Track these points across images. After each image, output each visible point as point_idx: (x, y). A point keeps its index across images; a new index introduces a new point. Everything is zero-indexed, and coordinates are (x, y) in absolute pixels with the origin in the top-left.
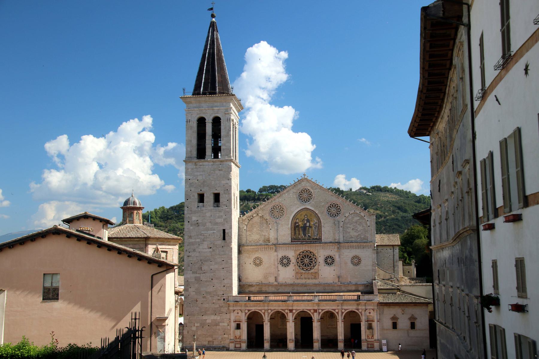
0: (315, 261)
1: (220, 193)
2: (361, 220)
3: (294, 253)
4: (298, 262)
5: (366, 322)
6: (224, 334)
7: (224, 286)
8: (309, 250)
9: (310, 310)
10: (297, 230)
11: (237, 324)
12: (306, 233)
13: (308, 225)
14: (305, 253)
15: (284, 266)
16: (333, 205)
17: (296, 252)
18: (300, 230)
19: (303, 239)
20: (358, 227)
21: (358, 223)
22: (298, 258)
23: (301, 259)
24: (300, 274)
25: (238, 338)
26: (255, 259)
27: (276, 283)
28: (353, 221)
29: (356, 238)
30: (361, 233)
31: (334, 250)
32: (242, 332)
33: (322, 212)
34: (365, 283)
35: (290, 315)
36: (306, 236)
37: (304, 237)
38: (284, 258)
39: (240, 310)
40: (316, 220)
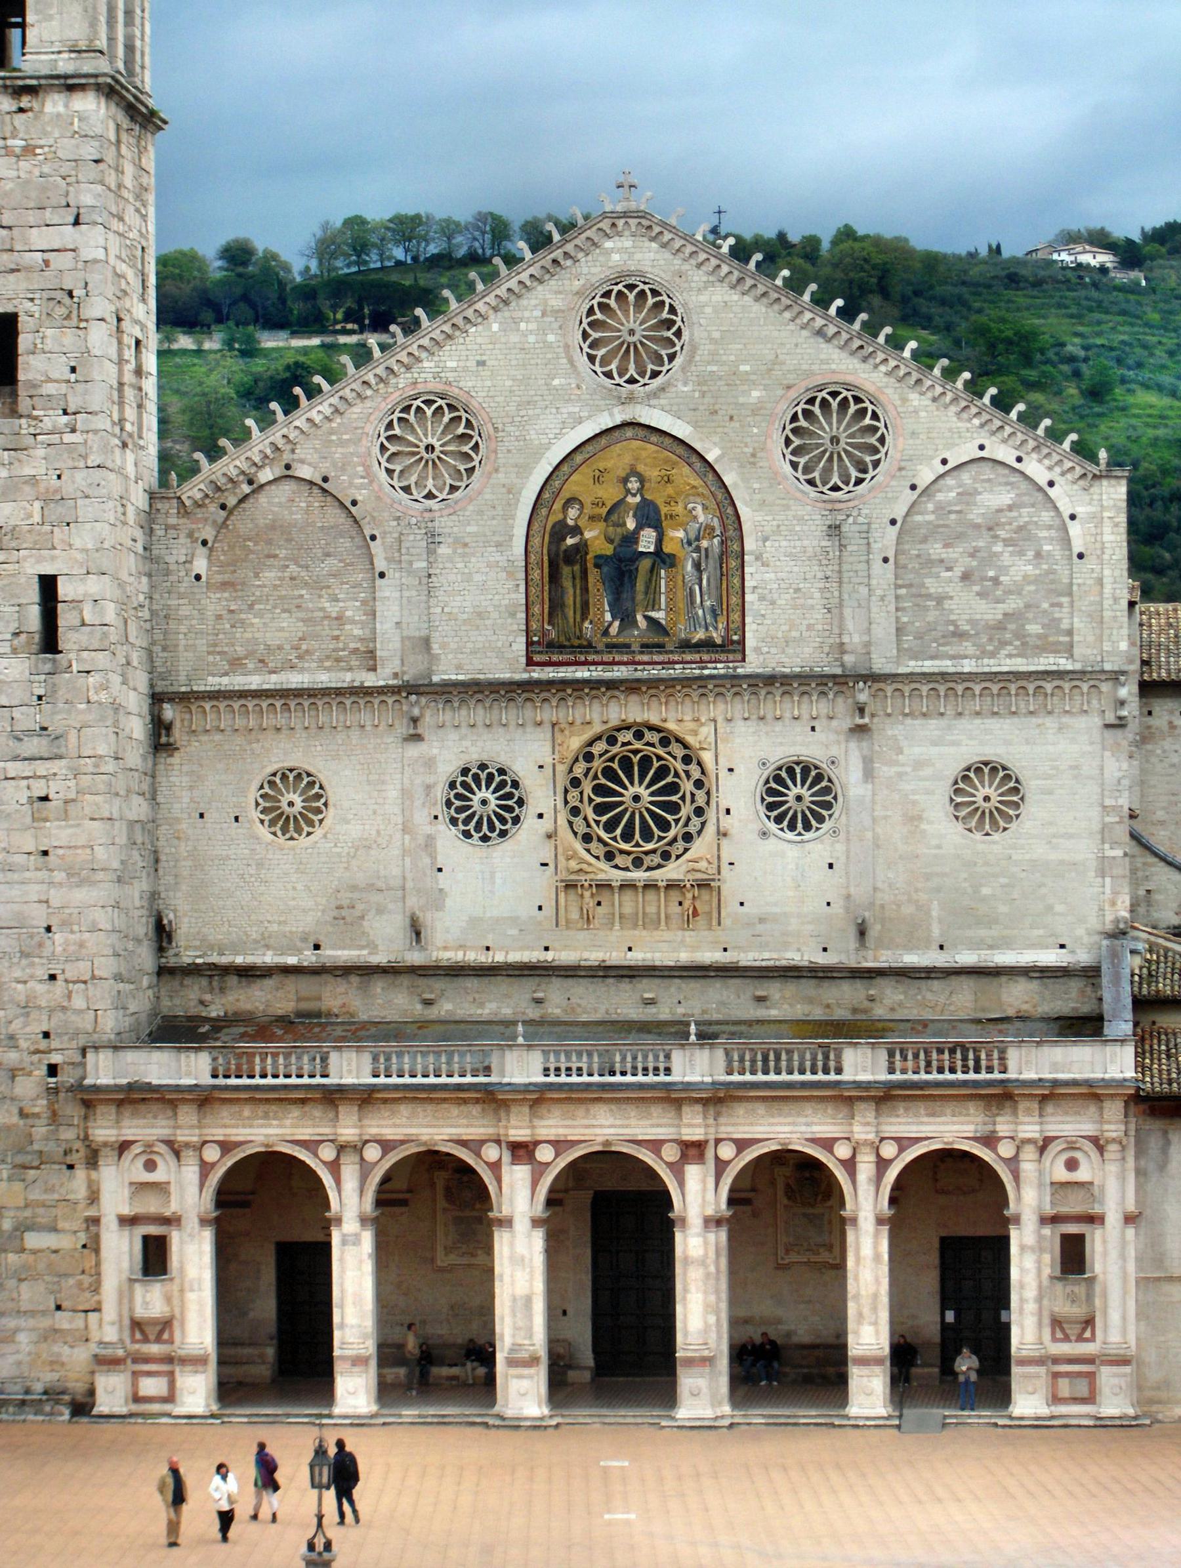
0: (693, 801)
1: (22, 318)
2: (1024, 511)
3: (548, 745)
4: (575, 811)
5: (1047, 1231)
6: (59, 1308)
7: (53, 977)
8: (655, 720)
9: (655, 1146)
10: (567, 584)
11: (146, 1239)
12: (633, 599)
13: (652, 549)
14: (624, 744)
15: (476, 836)
16: (825, 404)
17: (559, 738)
18: (591, 580)
19: (611, 647)
20: (1006, 559)
21: (1002, 533)
22: (576, 782)
23: (599, 790)
24: (587, 894)
25: (152, 1337)
26: (272, 784)
27: (415, 958)
28: (970, 516)
29: (991, 640)
30: (1028, 606)
31: (835, 723)
32: (182, 1291)
33: (749, 450)
34: (1050, 957)
35: (517, 1177)
36: (634, 623)
37: (621, 629)
38: (476, 778)
39: (169, 1143)
40: (705, 508)
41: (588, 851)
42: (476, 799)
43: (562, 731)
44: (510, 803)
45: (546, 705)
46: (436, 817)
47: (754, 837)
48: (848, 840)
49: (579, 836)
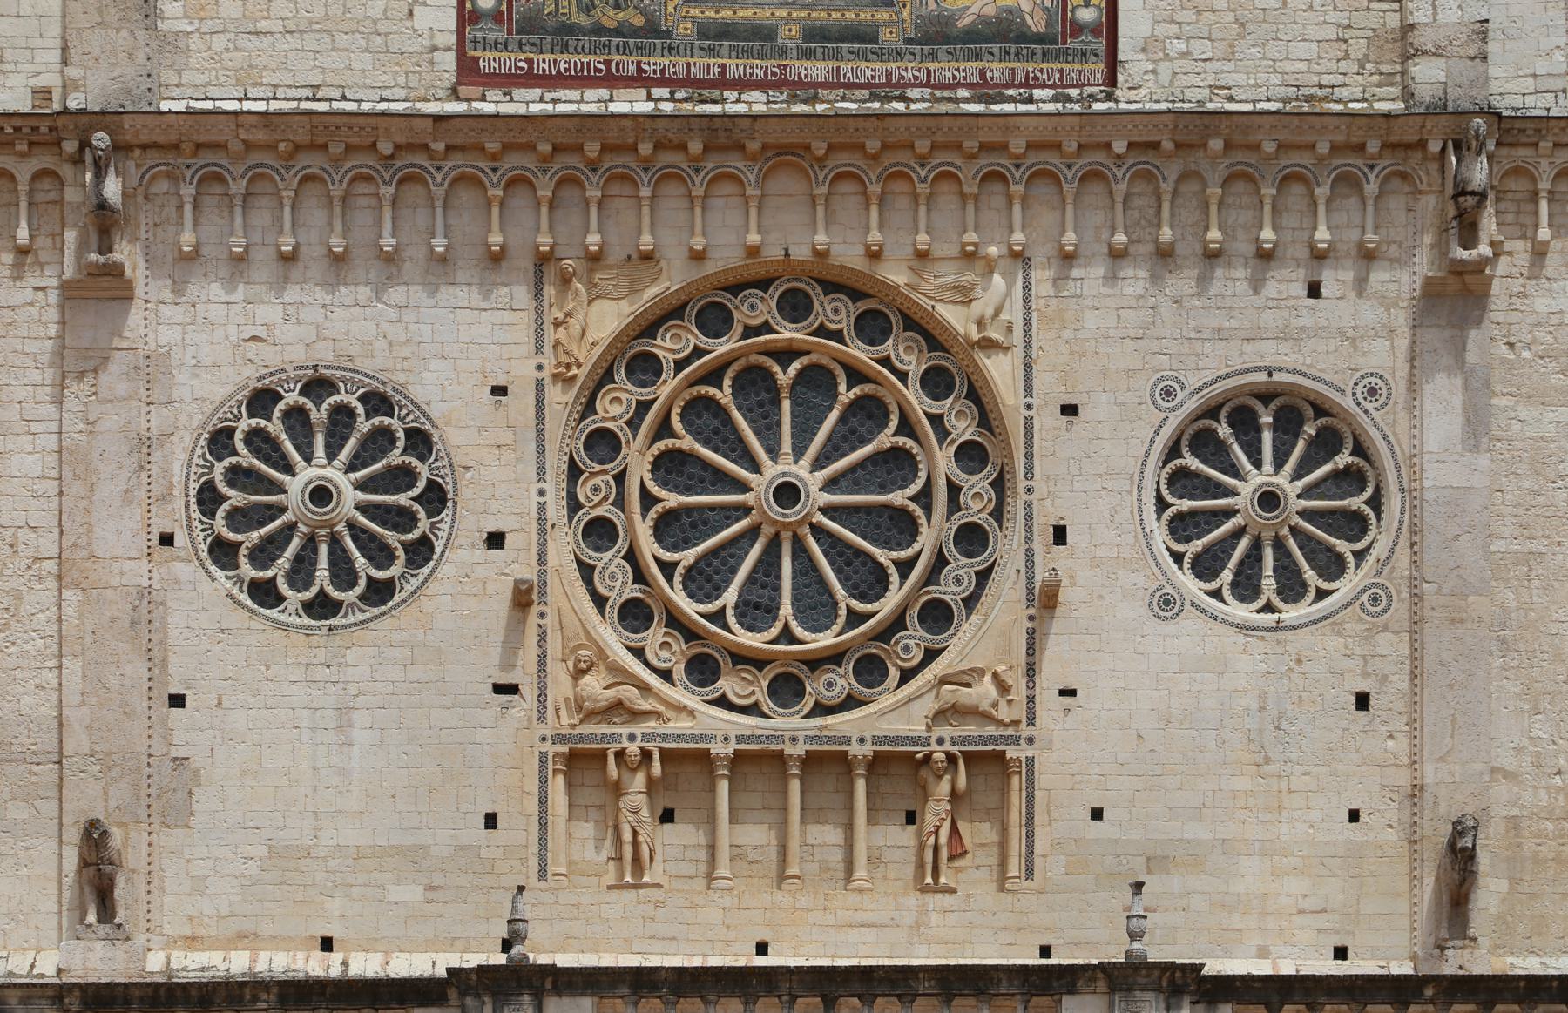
8: (848, 255)
14: (749, 332)
15: (294, 598)
22: (603, 443)
41: (639, 653)
42: (296, 486)
43: (565, 280)
44: (402, 499)
45: (520, 200)
46: (167, 540)
47: (1135, 611)
48: (1416, 625)
49: (612, 609)
